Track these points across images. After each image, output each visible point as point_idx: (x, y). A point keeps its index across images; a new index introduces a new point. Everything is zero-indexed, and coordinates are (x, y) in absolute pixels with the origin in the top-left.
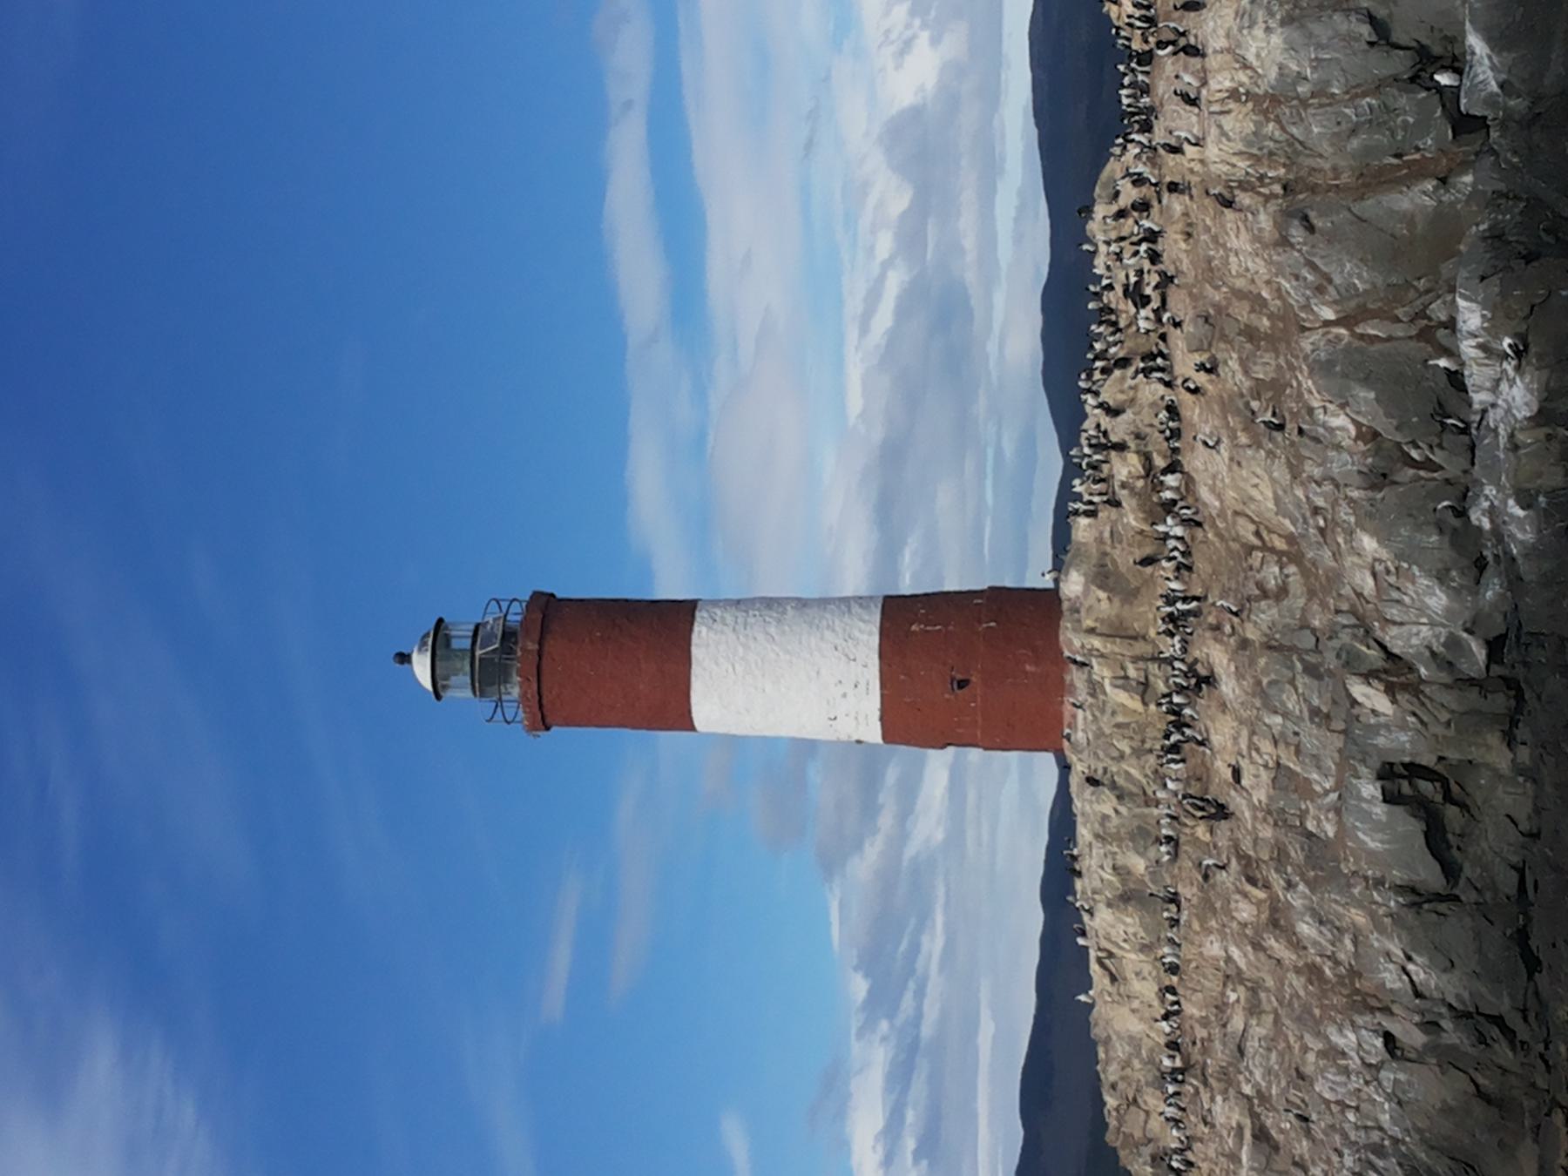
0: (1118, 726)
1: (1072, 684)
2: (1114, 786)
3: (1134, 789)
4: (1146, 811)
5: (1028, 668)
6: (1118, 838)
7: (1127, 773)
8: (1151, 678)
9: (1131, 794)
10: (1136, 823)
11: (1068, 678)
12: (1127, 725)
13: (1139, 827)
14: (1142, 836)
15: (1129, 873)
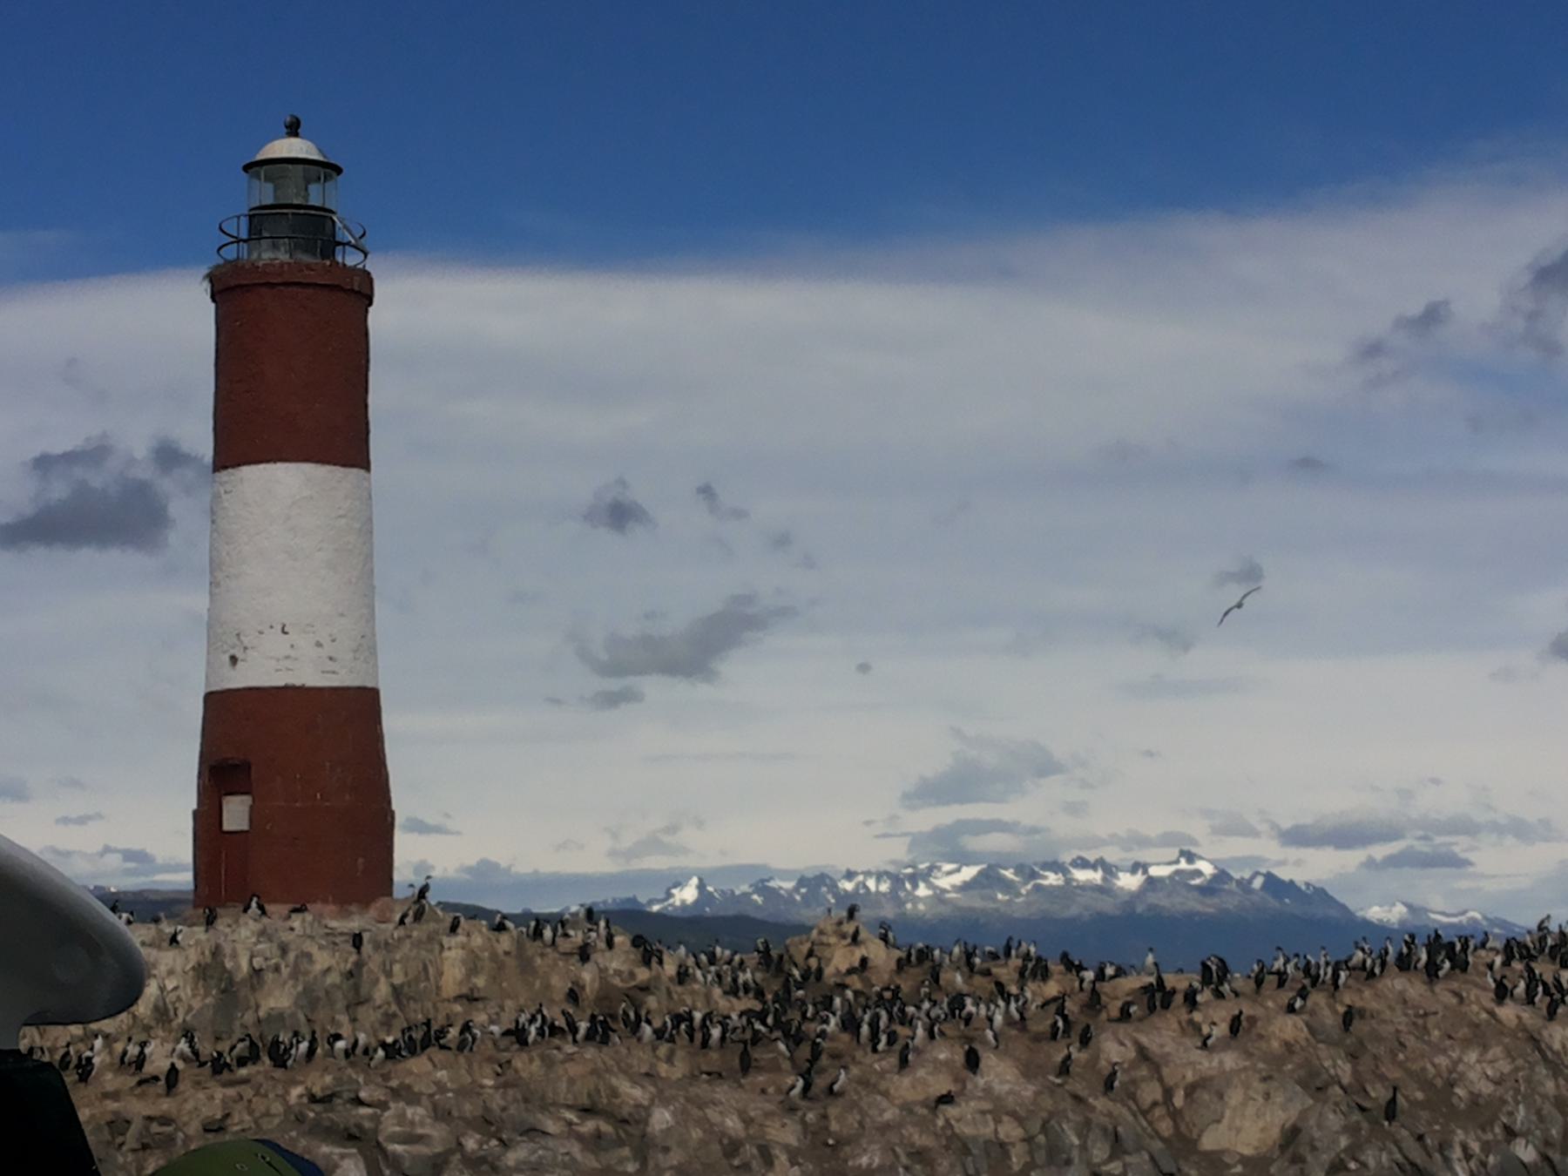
0: (425, 968)
1: (351, 913)
2: (359, 965)
3: (364, 991)
4: (340, 1005)
5: (361, 860)
6: (295, 974)
7: (377, 981)
8: (480, 1005)
9: (356, 988)
10: (322, 994)
11: (353, 908)
12: (427, 979)
13: (318, 999)
14: (310, 999)
15: (253, 989)
